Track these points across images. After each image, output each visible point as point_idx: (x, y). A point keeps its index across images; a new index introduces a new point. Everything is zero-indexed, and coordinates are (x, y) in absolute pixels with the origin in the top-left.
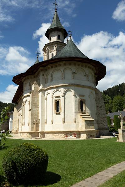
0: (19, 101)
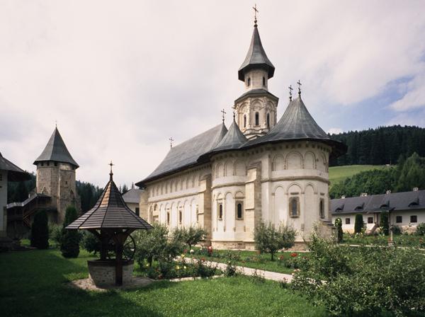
0: (153, 184)
